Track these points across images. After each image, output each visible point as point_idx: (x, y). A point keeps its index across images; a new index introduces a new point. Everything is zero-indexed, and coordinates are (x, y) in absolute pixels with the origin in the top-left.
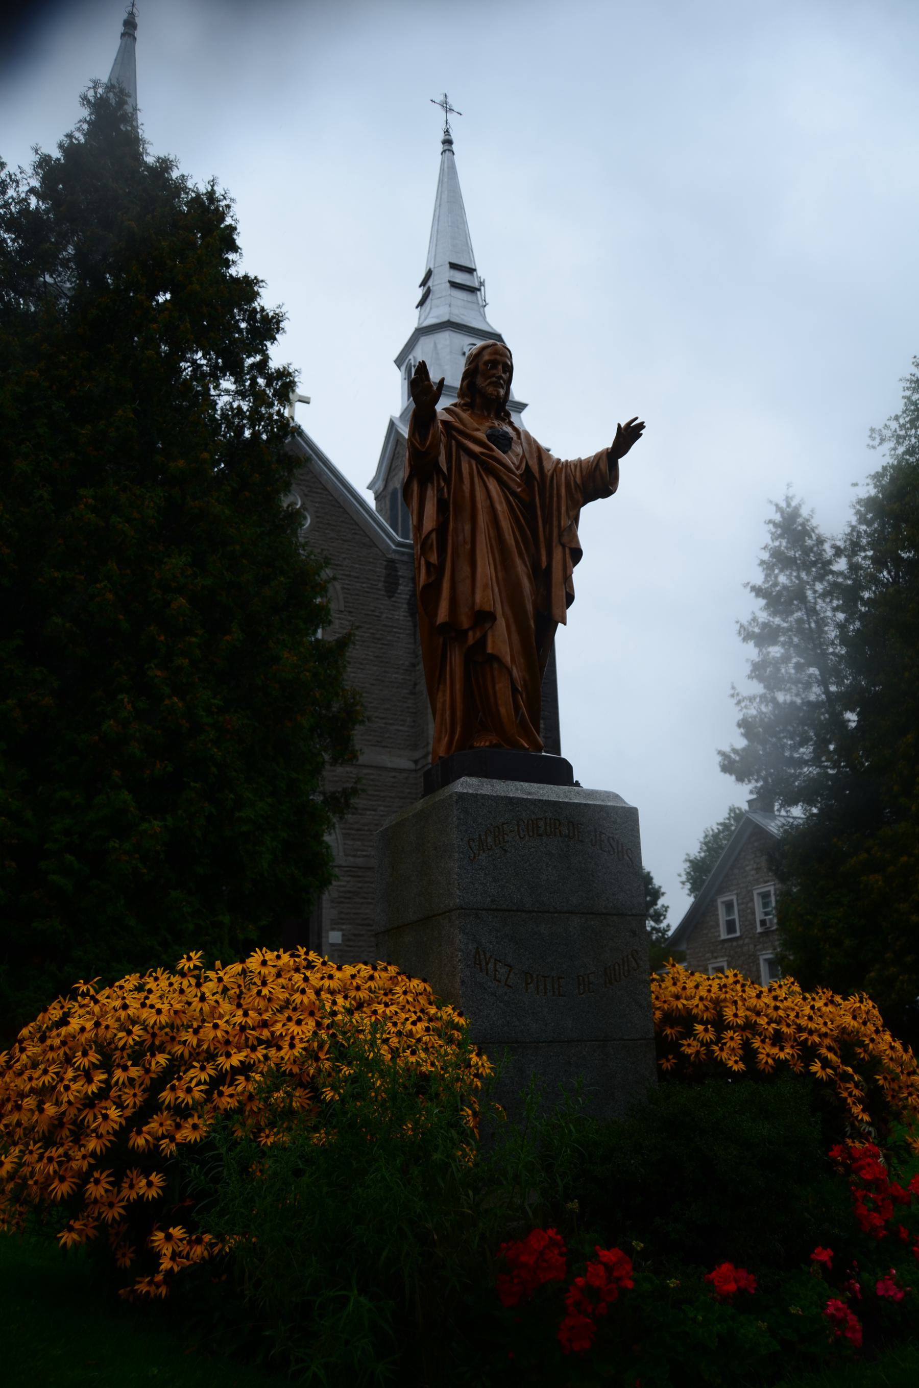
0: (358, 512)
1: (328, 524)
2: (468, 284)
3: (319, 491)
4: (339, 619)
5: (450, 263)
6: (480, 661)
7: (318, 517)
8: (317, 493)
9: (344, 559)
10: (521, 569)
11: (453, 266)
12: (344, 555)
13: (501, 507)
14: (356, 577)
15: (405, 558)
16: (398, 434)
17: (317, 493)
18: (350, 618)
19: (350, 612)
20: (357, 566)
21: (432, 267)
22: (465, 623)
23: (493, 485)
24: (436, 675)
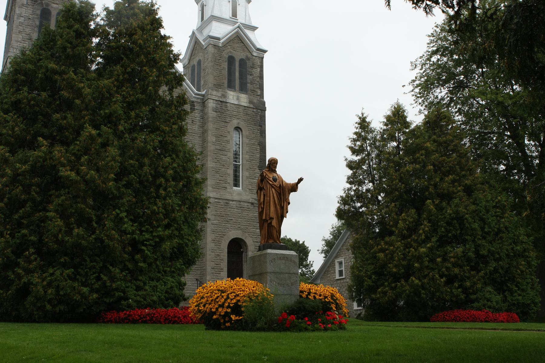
6: (270, 225)
10: (278, 207)
13: (275, 195)
15: (199, 100)
16: (196, 38)
22: (268, 218)
23: (273, 190)
24: (261, 228)
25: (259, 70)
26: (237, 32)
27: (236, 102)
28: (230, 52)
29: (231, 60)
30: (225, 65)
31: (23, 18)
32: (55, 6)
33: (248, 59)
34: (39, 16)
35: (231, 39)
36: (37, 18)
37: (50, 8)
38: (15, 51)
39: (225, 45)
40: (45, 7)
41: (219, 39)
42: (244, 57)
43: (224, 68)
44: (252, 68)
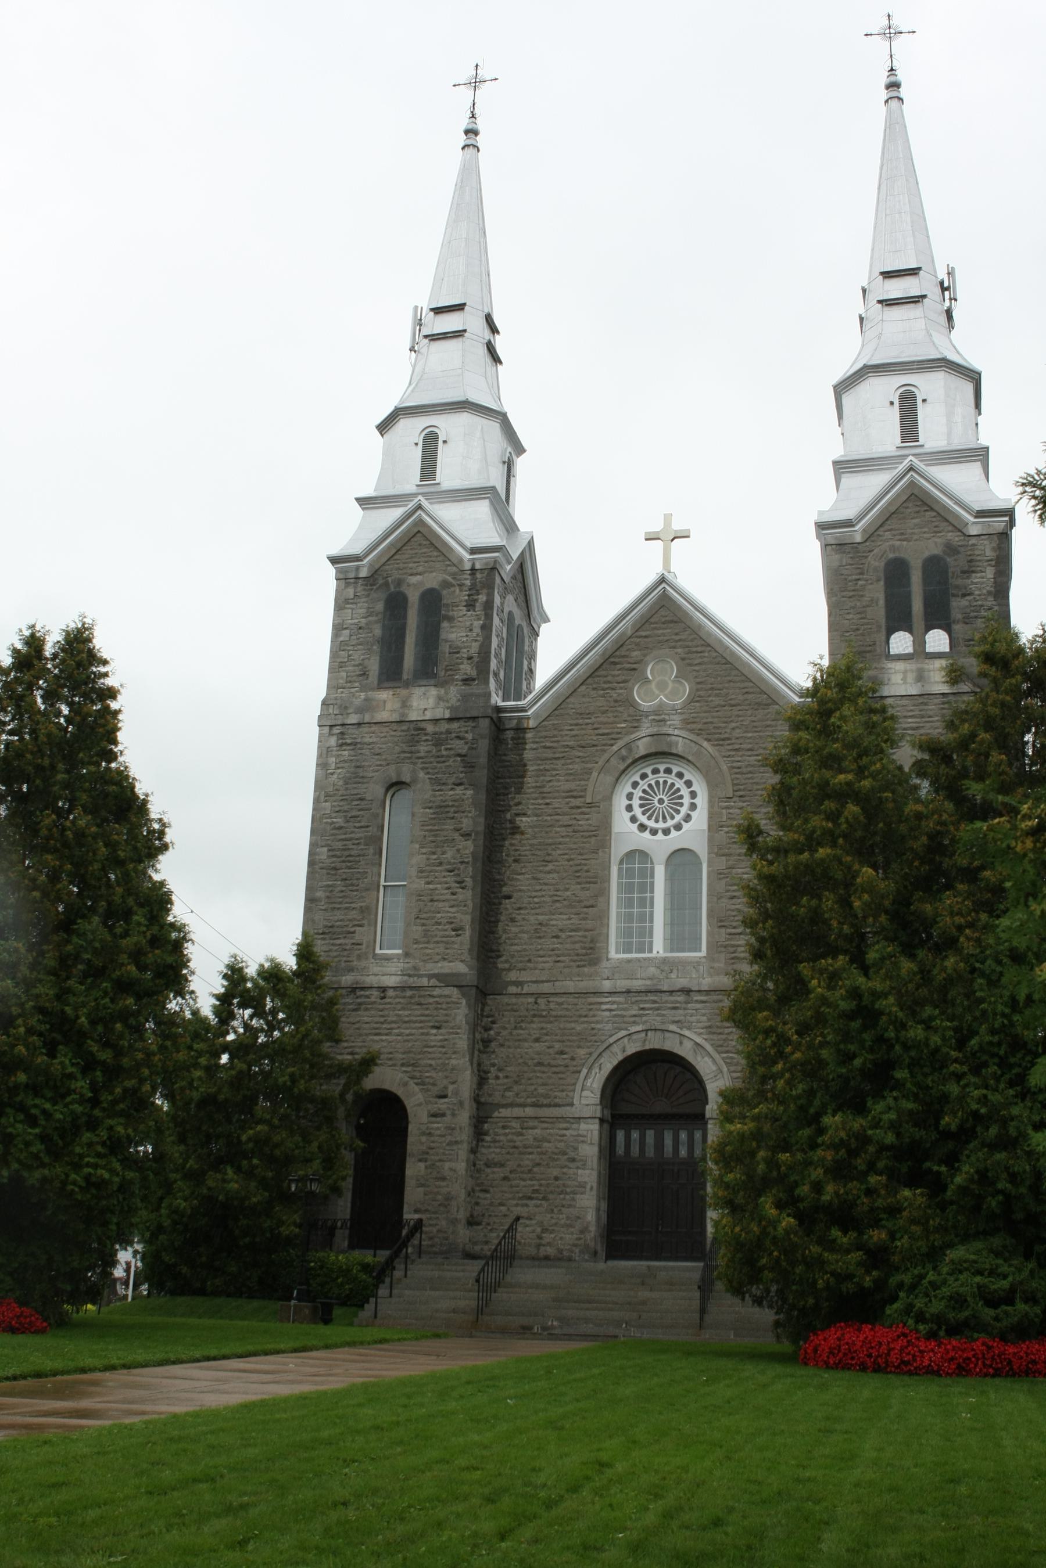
0: (748, 665)
1: (712, 689)
2: (915, 292)
3: (699, 649)
4: (727, 808)
5: (882, 273)
7: (698, 683)
8: (697, 652)
9: (733, 729)
11: (887, 275)
12: (734, 725)
14: (749, 750)
17: (697, 652)
18: (741, 804)
19: (741, 796)
20: (750, 735)
21: (865, 284)
25: (990, 572)
26: (912, 484)
27: (914, 691)
28: (893, 548)
29: (896, 572)
30: (877, 592)
31: (347, 632)
32: (414, 580)
33: (951, 549)
34: (380, 616)
35: (893, 509)
36: (376, 622)
37: (404, 588)
38: (331, 711)
39: (872, 534)
40: (392, 589)
41: (848, 523)
42: (937, 551)
43: (873, 601)
44: (967, 572)
